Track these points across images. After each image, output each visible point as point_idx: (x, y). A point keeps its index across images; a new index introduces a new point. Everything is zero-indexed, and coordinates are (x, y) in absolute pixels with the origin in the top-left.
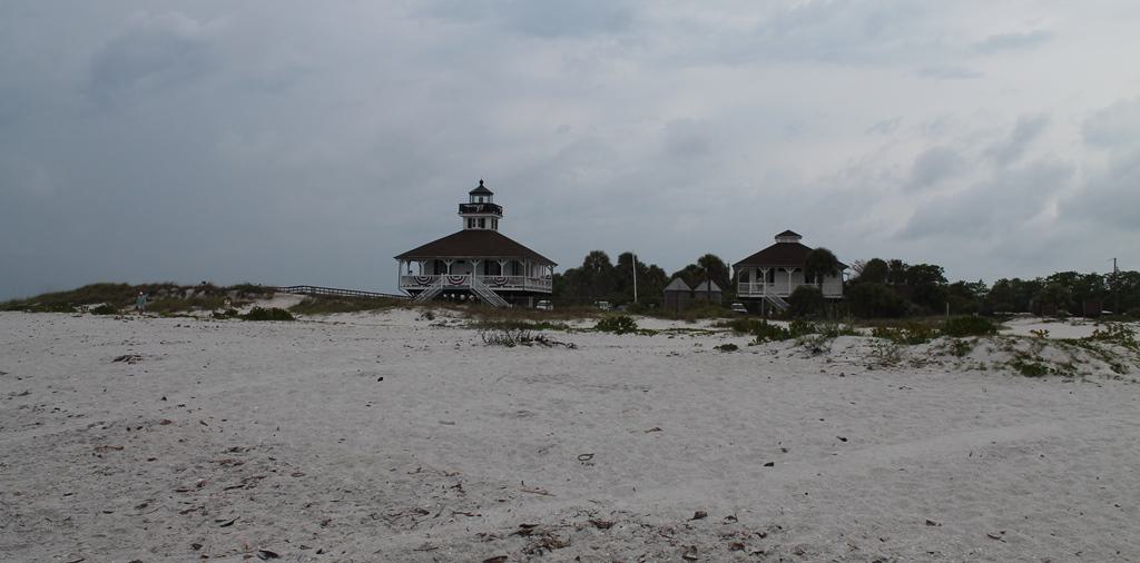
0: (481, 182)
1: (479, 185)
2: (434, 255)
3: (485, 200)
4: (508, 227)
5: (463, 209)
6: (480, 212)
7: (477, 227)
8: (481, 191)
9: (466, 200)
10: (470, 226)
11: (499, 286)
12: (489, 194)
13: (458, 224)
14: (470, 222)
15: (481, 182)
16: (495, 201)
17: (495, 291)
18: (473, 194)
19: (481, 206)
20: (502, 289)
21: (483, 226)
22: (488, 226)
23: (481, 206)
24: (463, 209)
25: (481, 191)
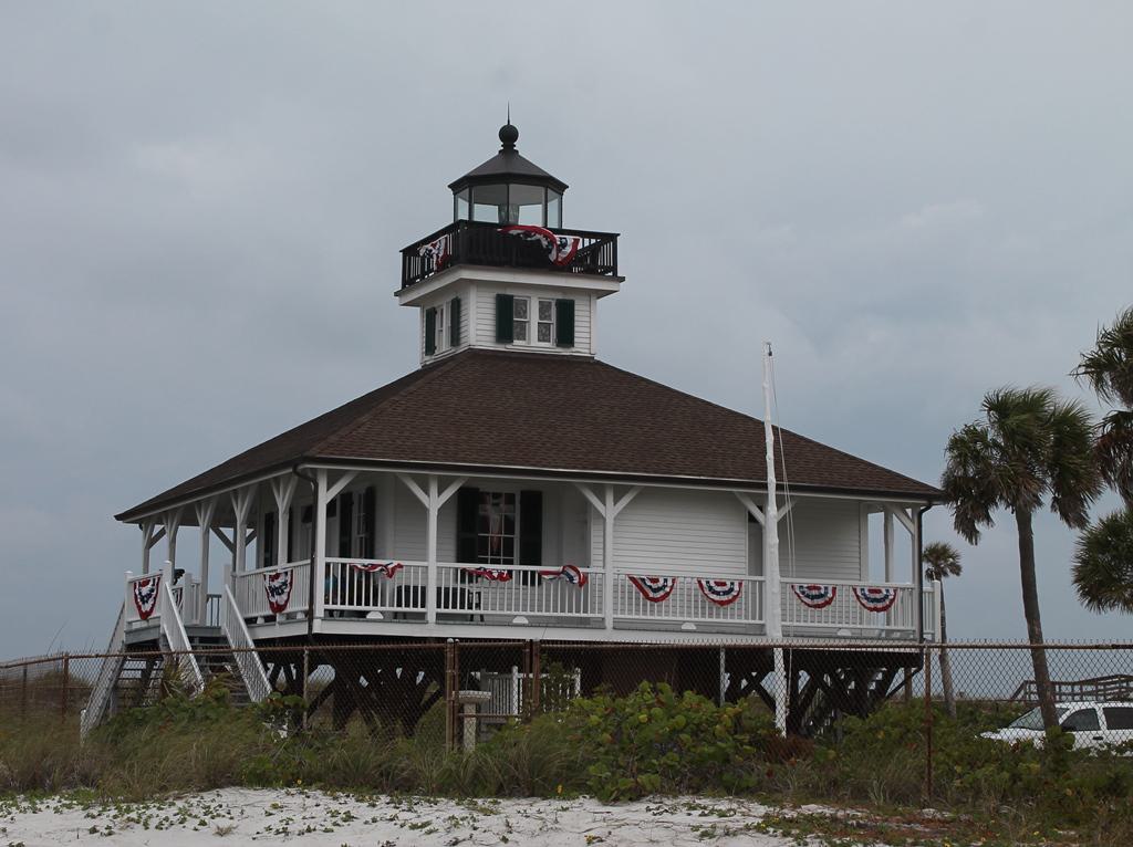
0: (509, 135)
1: (499, 145)
3: (529, 216)
7: (532, 342)
8: (507, 174)
15: (509, 135)
25: (507, 174)
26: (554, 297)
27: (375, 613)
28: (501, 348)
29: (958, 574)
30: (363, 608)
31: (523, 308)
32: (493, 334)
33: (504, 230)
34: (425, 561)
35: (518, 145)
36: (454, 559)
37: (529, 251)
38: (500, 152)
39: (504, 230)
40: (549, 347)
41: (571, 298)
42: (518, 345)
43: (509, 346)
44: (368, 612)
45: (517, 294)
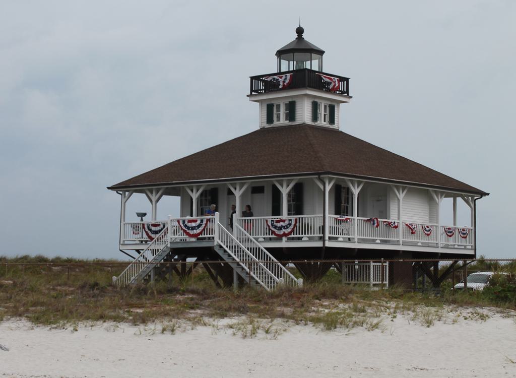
0: (300, 31)
1: (295, 36)
2: (201, 178)
4: (352, 120)
6: (287, 88)
7: (283, 121)
8: (300, 48)
10: (270, 119)
11: (279, 238)
13: (248, 118)
15: (300, 31)
16: (331, 65)
17: (282, 255)
20: (284, 244)
21: (291, 115)
22: (304, 115)
25: (300, 48)
26: (287, 101)
27: (305, 237)
30: (301, 236)
31: (278, 107)
32: (266, 121)
33: (300, 73)
34: (280, 215)
35: (304, 36)
36: (271, 214)
37: (316, 81)
38: (296, 38)
39: (300, 73)
40: (287, 123)
41: (293, 100)
42: (276, 123)
43: (272, 125)
44: (302, 237)
45: (275, 103)
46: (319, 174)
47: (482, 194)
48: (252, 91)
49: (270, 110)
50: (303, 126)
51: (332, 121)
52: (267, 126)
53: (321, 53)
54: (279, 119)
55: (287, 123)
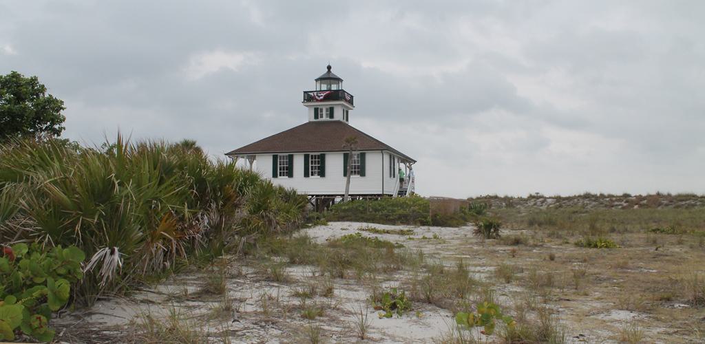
0: (329, 68)
3: (334, 87)
5: (308, 97)
7: (325, 118)
8: (329, 78)
9: (312, 86)
10: (316, 117)
12: (338, 80)
13: (304, 116)
14: (317, 112)
15: (329, 68)
18: (321, 80)
19: (330, 93)
21: (331, 116)
22: (338, 115)
23: (330, 93)
24: (308, 97)
25: (329, 78)
26: (328, 107)
28: (317, 120)
29: (305, 176)
31: (321, 110)
40: (328, 119)
42: (320, 119)
45: (320, 107)
46: (382, 150)
47: (415, 162)
48: (304, 100)
49: (316, 110)
50: (339, 122)
51: (347, 120)
52: (313, 119)
53: (342, 81)
54: (322, 117)
55: (328, 119)
